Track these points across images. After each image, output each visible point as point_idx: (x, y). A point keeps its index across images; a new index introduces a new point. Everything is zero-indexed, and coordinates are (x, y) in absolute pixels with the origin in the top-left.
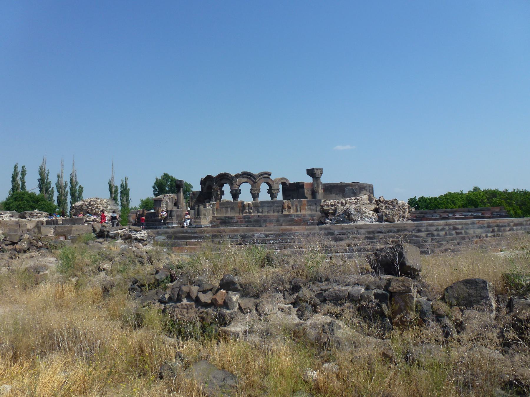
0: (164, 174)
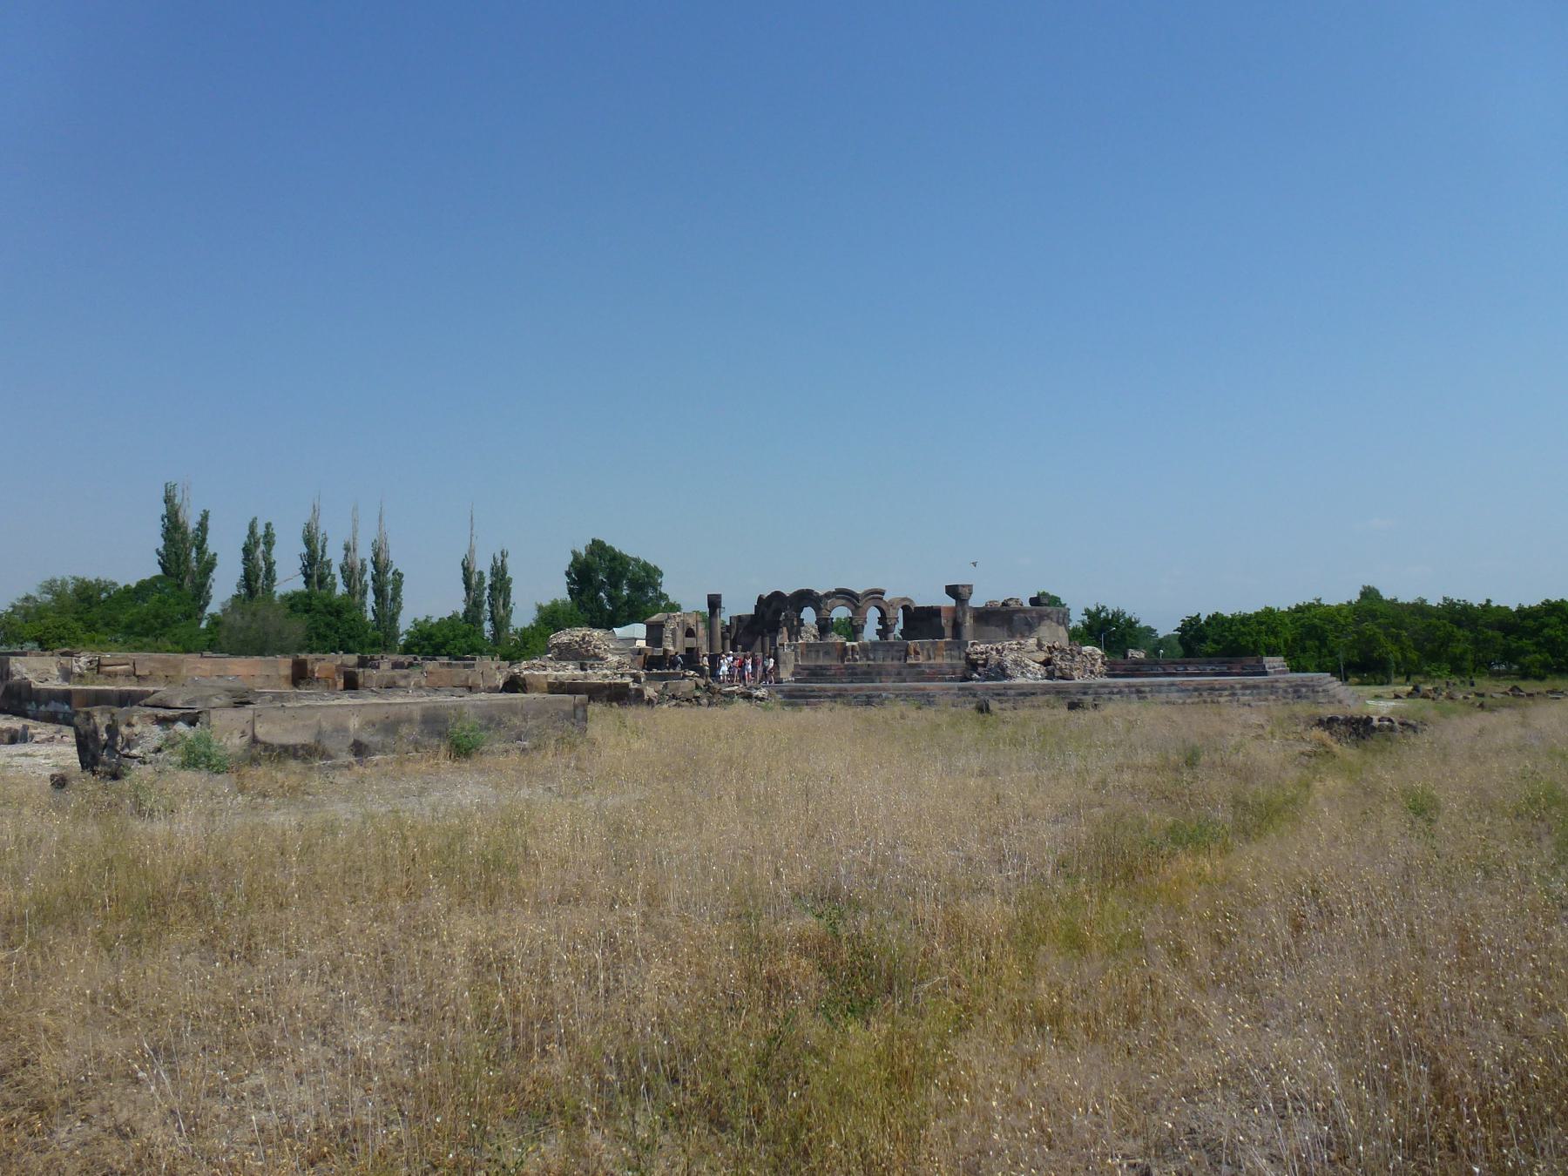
0: (593, 541)
